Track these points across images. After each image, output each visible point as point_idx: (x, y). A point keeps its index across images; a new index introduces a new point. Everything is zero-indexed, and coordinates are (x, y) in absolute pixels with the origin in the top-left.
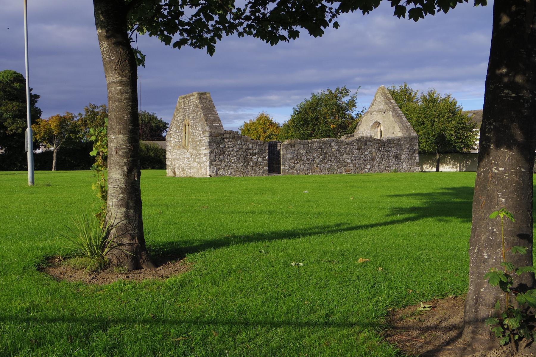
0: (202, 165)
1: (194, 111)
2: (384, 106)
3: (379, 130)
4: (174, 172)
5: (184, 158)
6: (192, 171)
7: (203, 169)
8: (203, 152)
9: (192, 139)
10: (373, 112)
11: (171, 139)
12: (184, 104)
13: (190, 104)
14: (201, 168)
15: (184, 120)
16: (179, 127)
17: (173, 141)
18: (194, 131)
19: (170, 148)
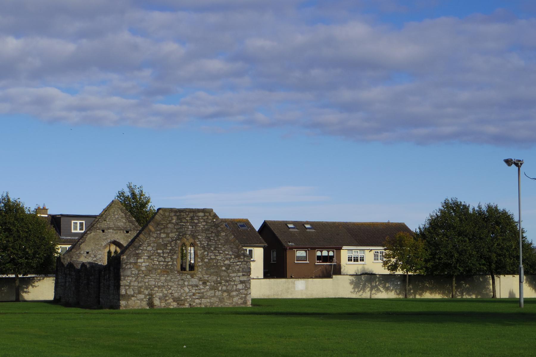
0: (234, 293)
1: (207, 230)
3: (107, 250)
4: (151, 304)
5: (182, 286)
7: (235, 299)
8: (237, 279)
9: (205, 263)
11: (139, 261)
12: (178, 219)
13: (196, 221)
14: (233, 297)
15: (178, 239)
16: (166, 245)
17: (144, 264)
18: (211, 254)
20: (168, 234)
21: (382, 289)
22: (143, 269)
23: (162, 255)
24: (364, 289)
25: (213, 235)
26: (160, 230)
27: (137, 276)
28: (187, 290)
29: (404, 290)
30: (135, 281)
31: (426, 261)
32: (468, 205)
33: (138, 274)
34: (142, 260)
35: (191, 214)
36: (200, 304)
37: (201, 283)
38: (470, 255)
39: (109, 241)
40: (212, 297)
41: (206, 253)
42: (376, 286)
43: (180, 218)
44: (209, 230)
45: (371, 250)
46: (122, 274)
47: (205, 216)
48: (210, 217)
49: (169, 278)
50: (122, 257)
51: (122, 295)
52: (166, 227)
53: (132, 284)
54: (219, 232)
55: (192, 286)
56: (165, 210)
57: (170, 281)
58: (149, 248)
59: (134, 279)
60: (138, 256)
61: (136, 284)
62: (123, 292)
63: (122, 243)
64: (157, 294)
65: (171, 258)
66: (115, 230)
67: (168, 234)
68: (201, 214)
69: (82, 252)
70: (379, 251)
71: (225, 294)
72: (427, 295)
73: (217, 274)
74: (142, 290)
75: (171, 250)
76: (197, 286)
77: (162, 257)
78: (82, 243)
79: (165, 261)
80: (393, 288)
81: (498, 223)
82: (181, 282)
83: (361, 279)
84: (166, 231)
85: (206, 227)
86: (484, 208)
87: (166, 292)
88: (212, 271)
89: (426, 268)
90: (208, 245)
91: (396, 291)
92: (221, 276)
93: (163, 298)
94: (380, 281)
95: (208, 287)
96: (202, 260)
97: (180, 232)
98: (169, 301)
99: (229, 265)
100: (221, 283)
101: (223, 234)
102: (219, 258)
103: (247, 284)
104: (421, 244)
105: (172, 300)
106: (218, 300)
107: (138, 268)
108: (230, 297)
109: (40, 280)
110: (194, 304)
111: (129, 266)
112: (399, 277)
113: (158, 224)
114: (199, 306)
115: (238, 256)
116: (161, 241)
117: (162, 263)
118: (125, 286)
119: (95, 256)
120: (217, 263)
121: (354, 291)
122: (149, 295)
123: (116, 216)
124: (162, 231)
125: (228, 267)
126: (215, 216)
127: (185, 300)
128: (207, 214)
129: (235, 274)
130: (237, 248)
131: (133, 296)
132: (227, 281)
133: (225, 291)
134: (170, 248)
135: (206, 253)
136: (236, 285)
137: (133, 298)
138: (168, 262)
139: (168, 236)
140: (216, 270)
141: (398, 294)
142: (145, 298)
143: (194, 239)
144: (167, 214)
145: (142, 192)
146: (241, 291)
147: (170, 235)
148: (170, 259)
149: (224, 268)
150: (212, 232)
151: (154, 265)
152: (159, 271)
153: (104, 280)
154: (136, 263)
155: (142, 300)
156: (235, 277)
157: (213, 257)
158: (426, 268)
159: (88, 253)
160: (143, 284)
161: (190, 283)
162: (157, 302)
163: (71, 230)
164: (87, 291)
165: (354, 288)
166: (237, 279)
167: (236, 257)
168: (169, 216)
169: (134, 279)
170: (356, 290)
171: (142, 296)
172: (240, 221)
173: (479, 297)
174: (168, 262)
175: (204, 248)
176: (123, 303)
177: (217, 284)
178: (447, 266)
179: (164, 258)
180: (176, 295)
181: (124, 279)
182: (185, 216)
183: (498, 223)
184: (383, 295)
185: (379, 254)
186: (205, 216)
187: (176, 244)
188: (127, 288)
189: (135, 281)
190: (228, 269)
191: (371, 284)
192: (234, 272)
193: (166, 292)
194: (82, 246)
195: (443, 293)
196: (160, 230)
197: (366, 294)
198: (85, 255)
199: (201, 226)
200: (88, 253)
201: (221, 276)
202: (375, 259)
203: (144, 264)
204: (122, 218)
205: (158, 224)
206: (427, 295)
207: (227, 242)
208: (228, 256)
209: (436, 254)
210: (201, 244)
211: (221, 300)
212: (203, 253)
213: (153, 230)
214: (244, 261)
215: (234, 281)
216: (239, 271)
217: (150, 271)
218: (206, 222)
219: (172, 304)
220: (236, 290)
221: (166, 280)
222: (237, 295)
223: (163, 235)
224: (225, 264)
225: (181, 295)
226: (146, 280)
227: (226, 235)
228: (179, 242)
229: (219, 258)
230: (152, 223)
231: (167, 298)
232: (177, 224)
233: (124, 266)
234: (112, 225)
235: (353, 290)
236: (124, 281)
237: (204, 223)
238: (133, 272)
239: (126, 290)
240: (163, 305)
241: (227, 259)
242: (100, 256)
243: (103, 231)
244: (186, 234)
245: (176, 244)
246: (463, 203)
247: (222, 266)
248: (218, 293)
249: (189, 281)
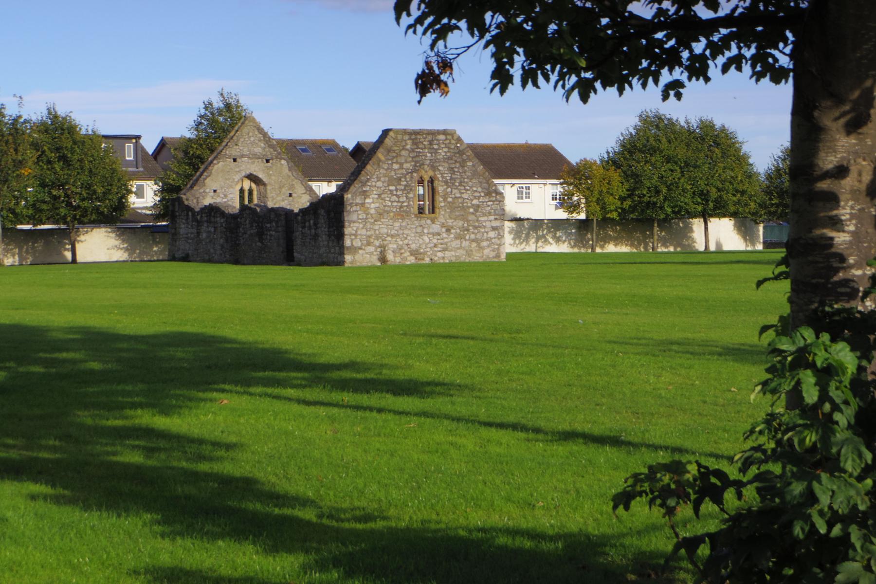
0: (485, 244)
1: (450, 158)
2: (264, 149)
3: (238, 187)
4: (383, 259)
5: (421, 234)
6: (447, 254)
7: (486, 251)
8: (488, 224)
9: (449, 203)
10: (242, 156)
11: (367, 201)
12: (414, 143)
13: (436, 147)
15: (415, 170)
16: (399, 179)
17: (373, 206)
18: (456, 191)
19: (362, 216)
20: (401, 164)
21: (551, 240)
22: (372, 211)
23: (395, 193)
24: (527, 239)
25: (458, 165)
26: (392, 159)
27: (365, 220)
28: (427, 240)
29: (580, 241)
30: (363, 228)
31: (622, 199)
32: (675, 119)
33: (367, 218)
34: (371, 200)
35: (430, 138)
36: (443, 258)
37: (444, 230)
38: (683, 190)
39: (244, 174)
40: (458, 248)
41: (449, 190)
42: (544, 236)
43: (415, 143)
44: (452, 159)
45: (514, 184)
46: (346, 219)
47: (446, 139)
48: (453, 142)
49: (404, 224)
50: (345, 196)
51: (348, 248)
52: (398, 155)
53: (359, 232)
54: (464, 161)
55: (433, 234)
56: (397, 132)
57: (406, 228)
58: (379, 184)
59: (361, 226)
60: (365, 194)
61: (364, 232)
62: (347, 242)
63: (260, 176)
64: (391, 246)
65: (407, 197)
66: (251, 158)
67: (401, 164)
68: (442, 137)
69: (207, 190)
70: (524, 186)
71: (474, 245)
72: (611, 248)
73: (464, 218)
74: (372, 240)
75: (405, 186)
76: (439, 234)
77: (396, 195)
78: (207, 177)
79: (399, 202)
80: (567, 237)
81: (717, 144)
82: (419, 230)
83: (524, 226)
84: (399, 160)
85: (448, 154)
86: (694, 123)
87: (401, 243)
88: (457, 213)
89: (622, 209)
90: (451, 178)
91: (570, 243)
92: (468, 221)
93: (398, 251)
94: (548, 228)
95: (452, 236)
96: (445, 200)
97: (416, 162)
98: (405, 255)
99: (478, 206)
100: (468, 230)
101: (470, 164)
102: (465, 196)
103: (501, 231)
104: (616, 176)
105: (408, 254)
106: (464, 253)
107: (366, 211)
108: (481, 248)
109: (87, 232)
110: (436, 259)
111: (354, 208)
112: (573, 224)
113: (389, 151)
114: (442, 261)
115: (488, 194)
116: (393, 173)
117: (395, 204)
118: (351, 235)
119: (226, 196)
120: (463, 203)
121: (515, 243)
122: (380, 246)
123: (252, 139)
124: (395, 160)
125: (477, 208)
126: (459, 140)
127: (425, 253)
128: (449, 137)
129: (485, 218)
130: (487, 183)
131: (360, 248)
132: (475, 227)
133: (473, 241)
134: (405, 183)
135: (449, 190)
136: (487, 233)
137: (360, 252)
138: (403, 202)
139: (401, 168)
140: (462, 213)
141: (572, 247)
142: (376, 251)
143: (434, 171)
144: (400, 137)
145: (238, 101)
146: (493, 241)
147: (405, 166)
148: (405, 199)
149: (471, 210)
150: (456, 161)
151: (385, 206)
152: (392, 214)
153: (304, 227)
154: (363, 204)
155: (371, 254)
156: (485, 221)
157: (458, 195)
158: (622, 209)
159: (215, 191)
160: (372, 232)
161: (431, 231)
162: (390, 256)
163: (124, 157)
164: (259, 244)
165: (514, 239)
166: (488, 224)
167: (486, 195)
168: (403, 140)
169: (361, 226)
170: (517, 242)
171: (371, 249)
172: (324, 143)
173: (679, 249)
174: (403, 202)
175: (446, 183)
176: (348, 258)
177: (464, 231)
178: (650, 205)
179: (398, 196)
180: (413, 246)
181: (349, 226)
182: (422, 140)
183: (717, 144)
184: (553, 247)
185: (524, 190)
186: (446, 139)
187: (412, 177)
188: (353, 237)
189: (363, 228)
190: (476, 211)
191: (536, 233)
192: (484, 215)
193: (401, 243)
194: (207, 181)
195: (632, 245)
196: (392, 159)
197: (531, 247)
198: (212, 194)
199: (443, 153)
200: (215, 191)
201: (468, 221)
202: (518, 198)
203: (373, 206)
204: (260, 141)
205: (389, 151)
206: (611, 248)
207: (475, 174)
208: (477, 194)
209: (634, 189)
210: (442, 177)
211: (469, 253)
212: (445, 190)
213: (383, 158)
214: (496, 200)
215: (485, 227)
216: (490, 213)
217: (381, 214)
218: (449, 148)
219: (409, 258)
220: (487, 240)
221: (401, 227)
222: (488, 246)
223: (396, 166)
224: (473, 205)
225: (420, 247)
226: (377, 227)
227: (473, 166)
228: (415, 175)
229: (465, 196)
230: (381, 150)
231: (403, 251)
232: (413, 150)
233: (349, 208)
234: (246, 151)
235: (512, 242)
236: (350, 229)
237: (446, 150)
238: (360, 217)
239: (352, 240)
240: (398, 260)
241: (475, 197)
242: (232, 196)
243: (235, 160)
244: (423, 164)
245: (412, 177)
246: (668, 116)
247: (469, 207)
248: (465, 244)
249: (429, 228)
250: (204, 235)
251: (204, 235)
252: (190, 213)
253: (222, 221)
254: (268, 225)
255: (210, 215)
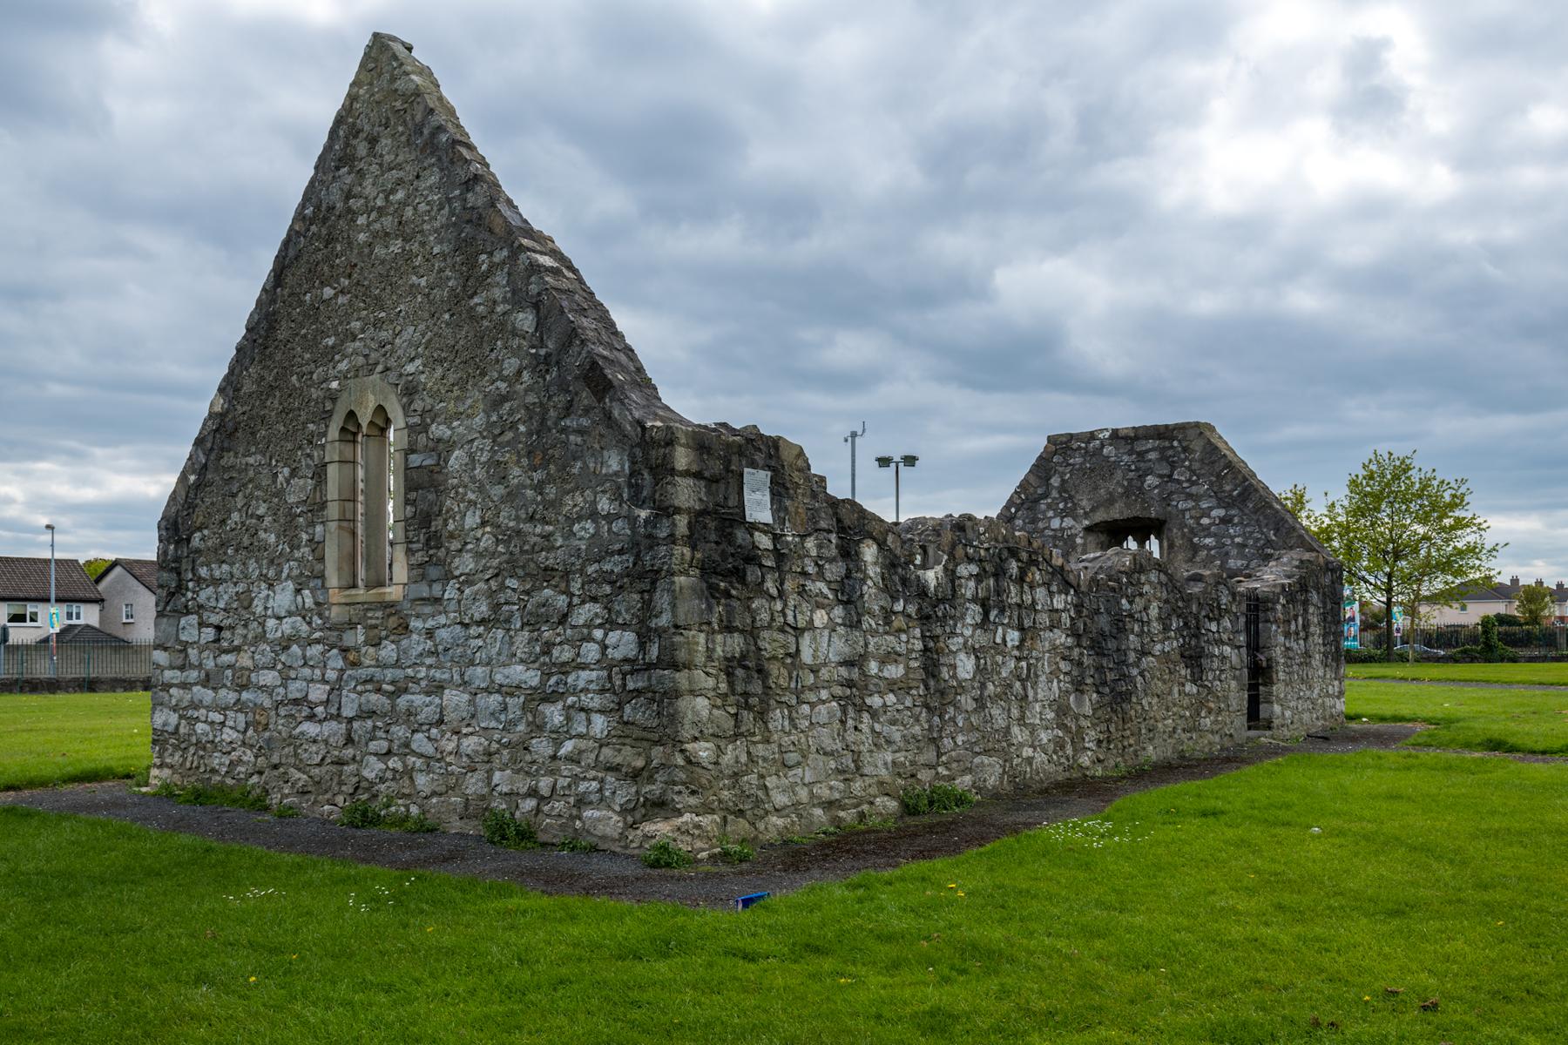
164: (1190, 688)
250: (966, 666)
251: (966, 666)
252: (869, 552)
253: (1059, 602)
254: (1214, 627)
255: (1000, 573)
